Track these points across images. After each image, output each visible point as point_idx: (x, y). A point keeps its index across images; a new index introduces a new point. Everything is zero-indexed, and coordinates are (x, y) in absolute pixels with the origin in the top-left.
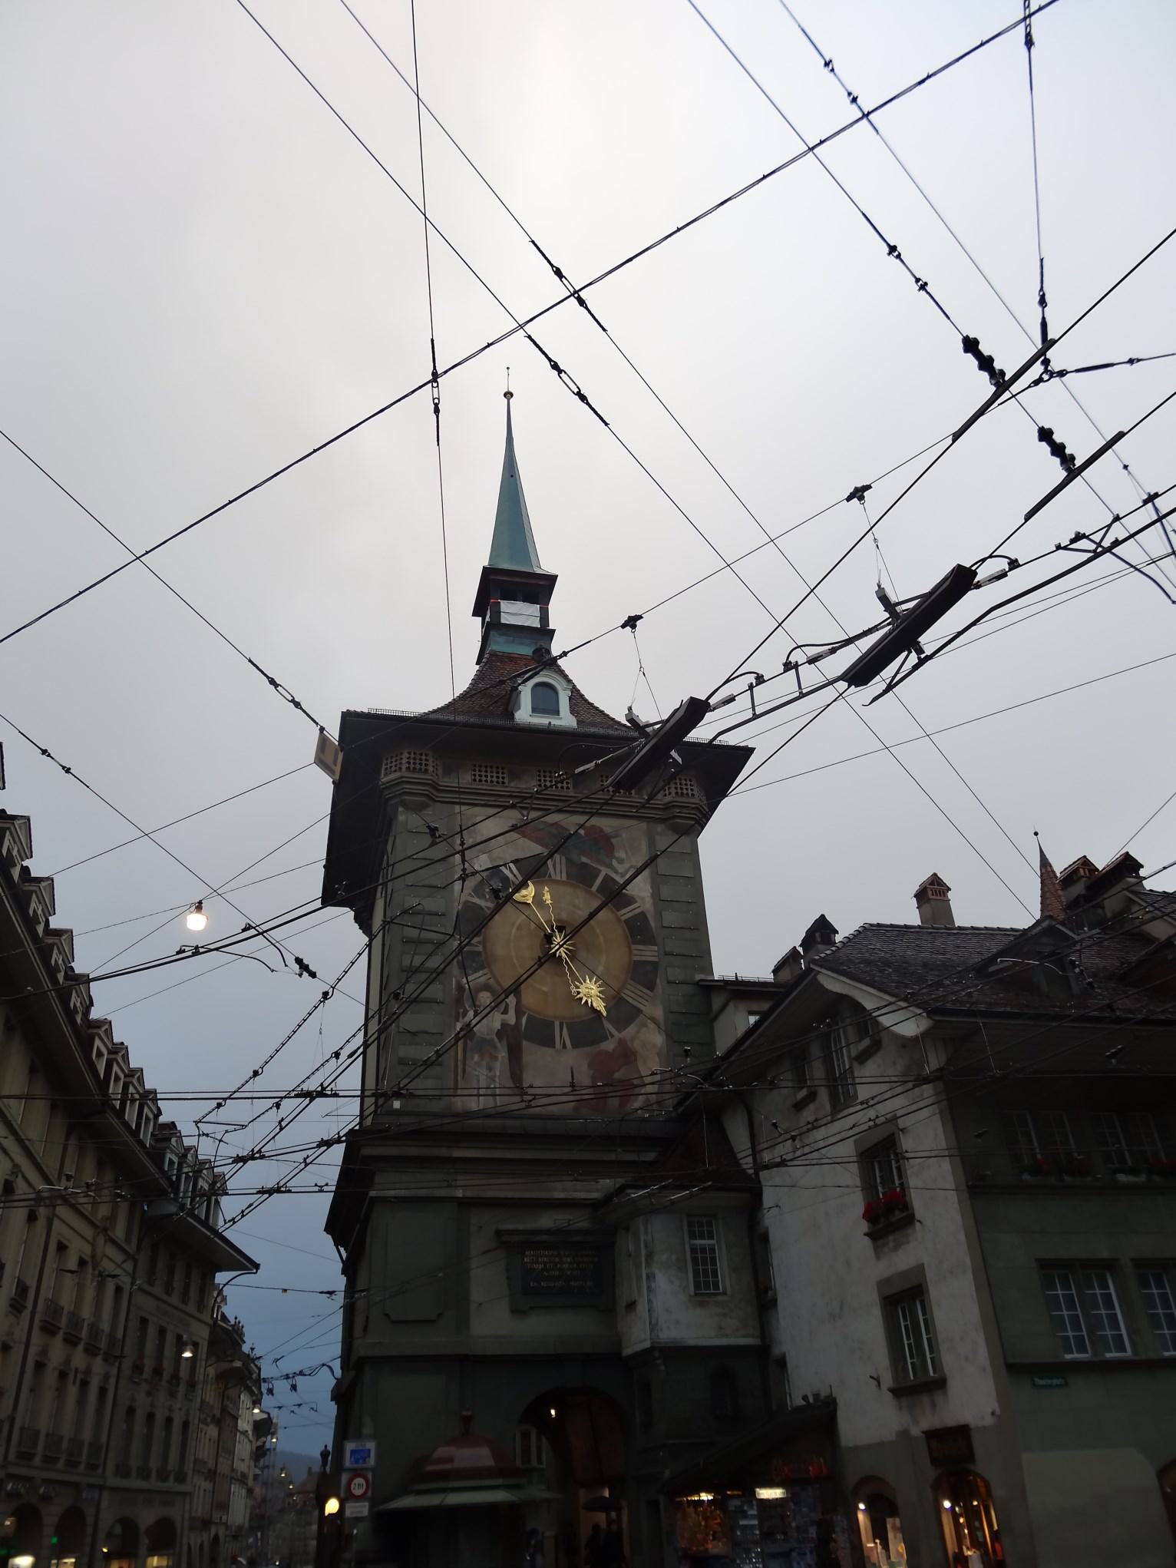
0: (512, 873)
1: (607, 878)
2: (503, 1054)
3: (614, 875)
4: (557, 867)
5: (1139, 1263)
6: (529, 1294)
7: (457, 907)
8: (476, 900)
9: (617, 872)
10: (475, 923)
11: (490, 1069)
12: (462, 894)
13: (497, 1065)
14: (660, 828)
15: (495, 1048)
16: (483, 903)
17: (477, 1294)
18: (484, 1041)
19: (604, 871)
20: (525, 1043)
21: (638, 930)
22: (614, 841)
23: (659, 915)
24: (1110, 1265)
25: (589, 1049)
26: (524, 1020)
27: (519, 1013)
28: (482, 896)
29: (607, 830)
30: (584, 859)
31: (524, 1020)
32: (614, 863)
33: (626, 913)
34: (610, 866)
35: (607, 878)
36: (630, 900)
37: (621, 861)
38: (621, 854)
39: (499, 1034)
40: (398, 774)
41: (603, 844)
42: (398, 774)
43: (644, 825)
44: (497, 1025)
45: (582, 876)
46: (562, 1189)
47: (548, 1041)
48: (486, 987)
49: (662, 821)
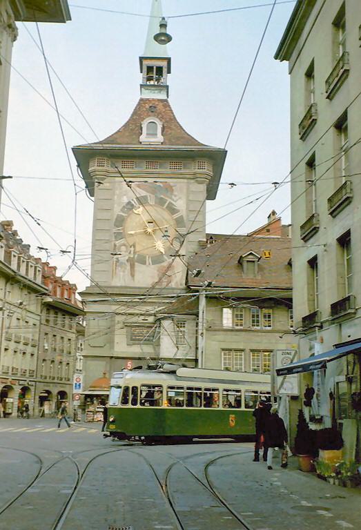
0: (135, 202)
1: (170, 203)
2: (128, 267)
3: (172, 201)
4: (152, 201)
5: (252, 351)
6: (133, 340)
7: (115, 217)
8: (122, 214)
9: (173, 200)
10: (120, 221)
11: (124, 272)
12: (117, 210)
13: (126, 273)
14: (192, 181)
15: (125, 264)
16: (123, 214)
17: (117, 339)
18: (122, 263)
19: (169, 200)
20: (136, 264)
21: (179, 222)
22: (174, 188)
23: (188, 216)
24: (242, 350)
25: (157, 265)
26: (136, 256)
27: (135, 253)
28: (123, 212)
29: (171, 184)
30: (162, 196)
31: (136, 256)
32: (173, 197)
33: (175, 216)
34: (171, 198)
35: (170, 203)
36: (178, 211)
37: (175, 196)
38: (175, 193)
39: (127, 261)
40: (93, 168)
41: (169, 189)
42: (93, 168)
43: (185, 180)
44: (127, 258)
45: (161, 202)
46: (144, 309)
47: (144, 263)
48: (124, 245)
49: (194, 179)
